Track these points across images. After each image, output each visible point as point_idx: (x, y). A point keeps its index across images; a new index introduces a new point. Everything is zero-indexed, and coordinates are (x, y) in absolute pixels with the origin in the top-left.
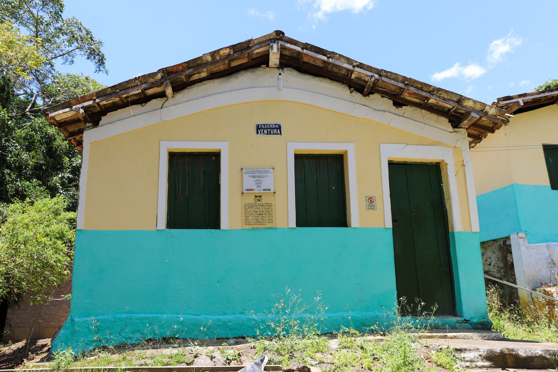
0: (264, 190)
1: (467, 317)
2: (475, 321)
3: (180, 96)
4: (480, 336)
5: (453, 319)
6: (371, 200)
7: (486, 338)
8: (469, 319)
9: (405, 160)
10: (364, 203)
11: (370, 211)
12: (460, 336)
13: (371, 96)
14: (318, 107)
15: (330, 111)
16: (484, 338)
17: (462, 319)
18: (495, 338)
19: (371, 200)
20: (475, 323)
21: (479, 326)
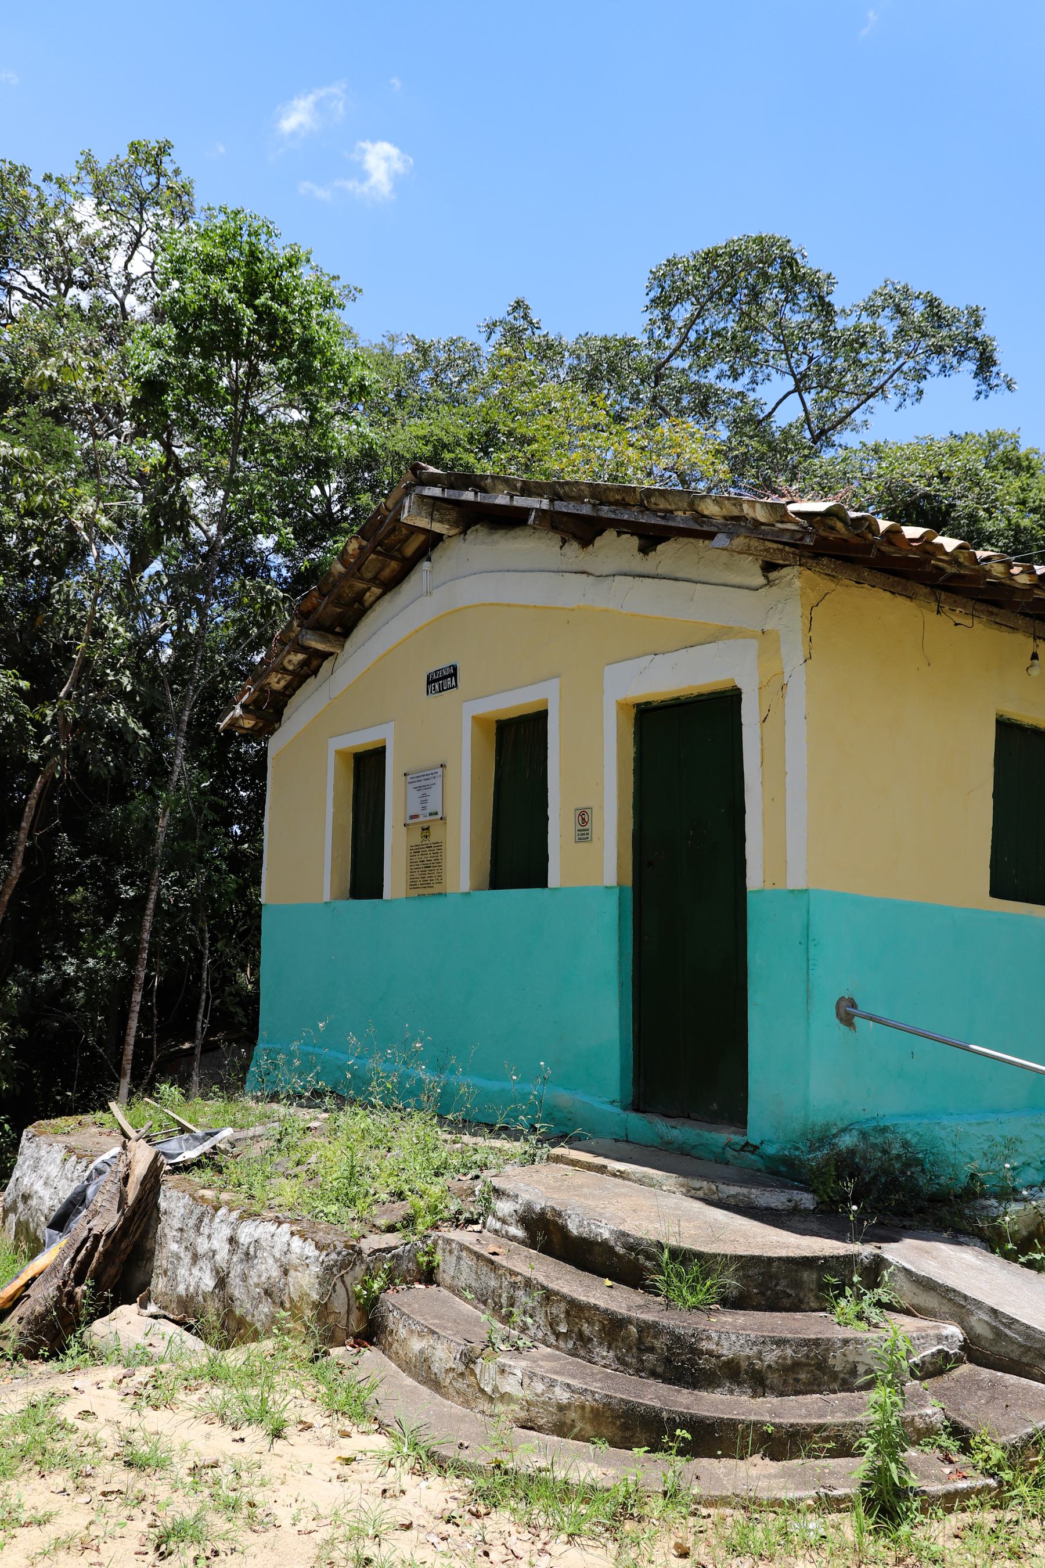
0: (431, 814)
1: (753, 1135)
2: (771, 1150)
3: (348, 644)
4: (682, 1186)
5: (722, 1137)
6: (583, 817)
7: (700, 1194)
8: (757, 1143)
9: (676, 695)
10: (571, 825)
11: (583, 846)
12: (634, 1173)
13: (598, 539)
14: (509, 605)
15: (527, 607)
16: (691, 1193)
17: (738, 1139)
18: (732, 1201)
19: (583, 817)
20: (771, 1158)
21: (783, 1169)
